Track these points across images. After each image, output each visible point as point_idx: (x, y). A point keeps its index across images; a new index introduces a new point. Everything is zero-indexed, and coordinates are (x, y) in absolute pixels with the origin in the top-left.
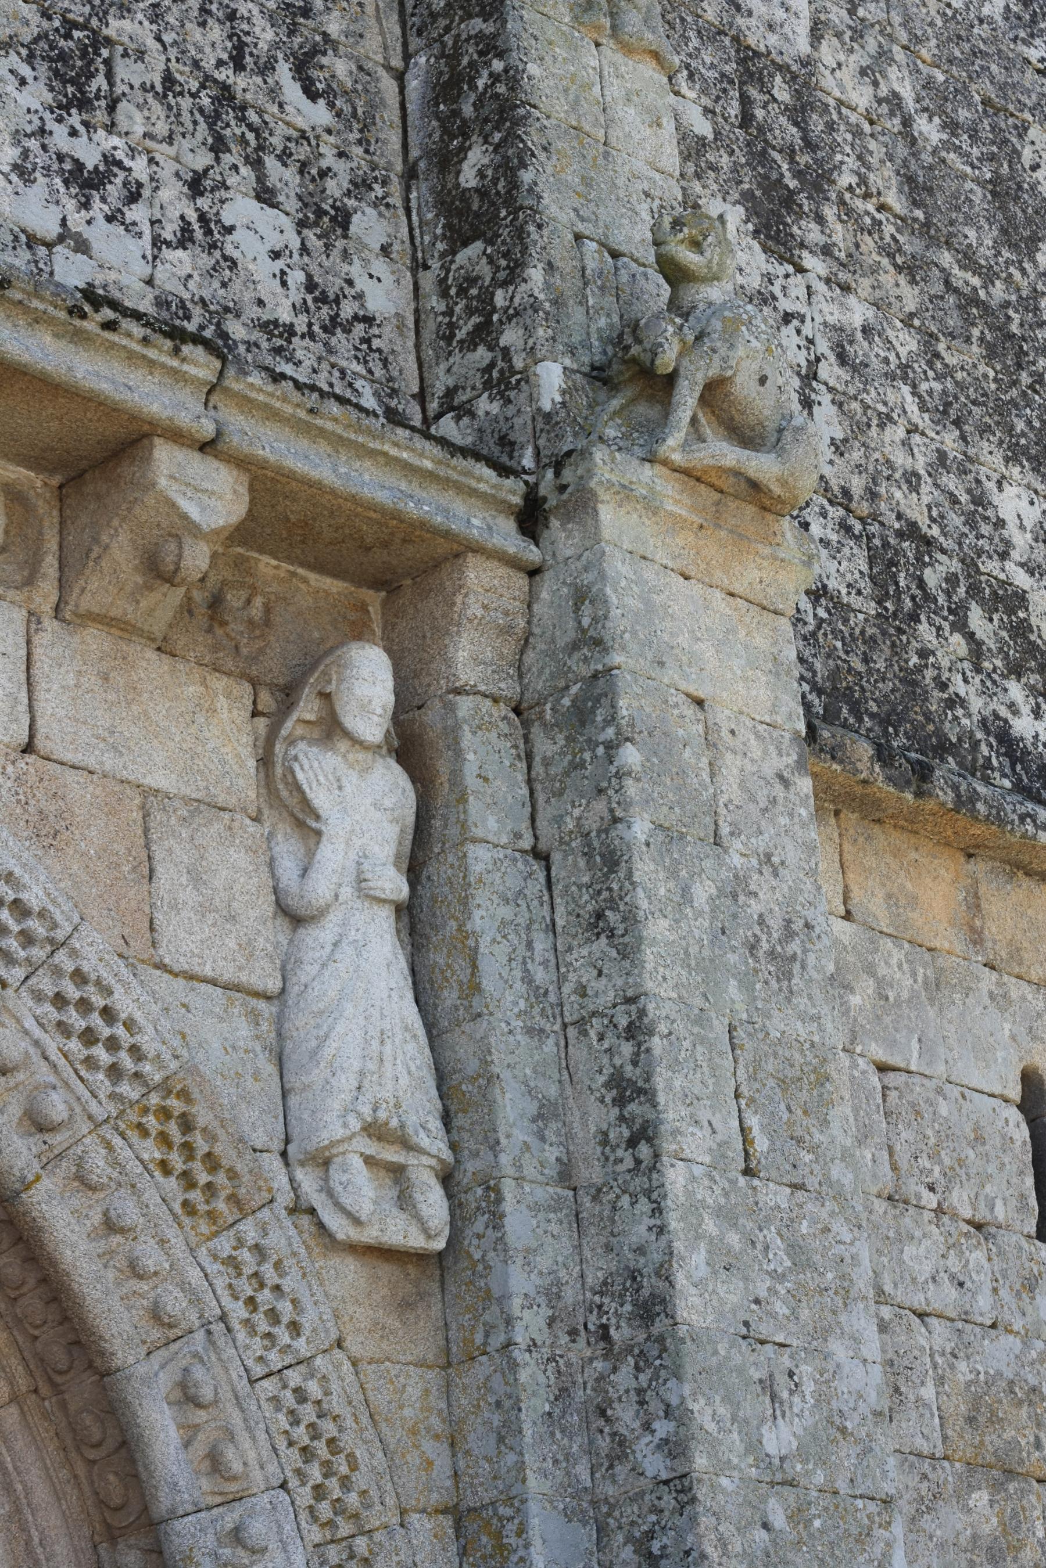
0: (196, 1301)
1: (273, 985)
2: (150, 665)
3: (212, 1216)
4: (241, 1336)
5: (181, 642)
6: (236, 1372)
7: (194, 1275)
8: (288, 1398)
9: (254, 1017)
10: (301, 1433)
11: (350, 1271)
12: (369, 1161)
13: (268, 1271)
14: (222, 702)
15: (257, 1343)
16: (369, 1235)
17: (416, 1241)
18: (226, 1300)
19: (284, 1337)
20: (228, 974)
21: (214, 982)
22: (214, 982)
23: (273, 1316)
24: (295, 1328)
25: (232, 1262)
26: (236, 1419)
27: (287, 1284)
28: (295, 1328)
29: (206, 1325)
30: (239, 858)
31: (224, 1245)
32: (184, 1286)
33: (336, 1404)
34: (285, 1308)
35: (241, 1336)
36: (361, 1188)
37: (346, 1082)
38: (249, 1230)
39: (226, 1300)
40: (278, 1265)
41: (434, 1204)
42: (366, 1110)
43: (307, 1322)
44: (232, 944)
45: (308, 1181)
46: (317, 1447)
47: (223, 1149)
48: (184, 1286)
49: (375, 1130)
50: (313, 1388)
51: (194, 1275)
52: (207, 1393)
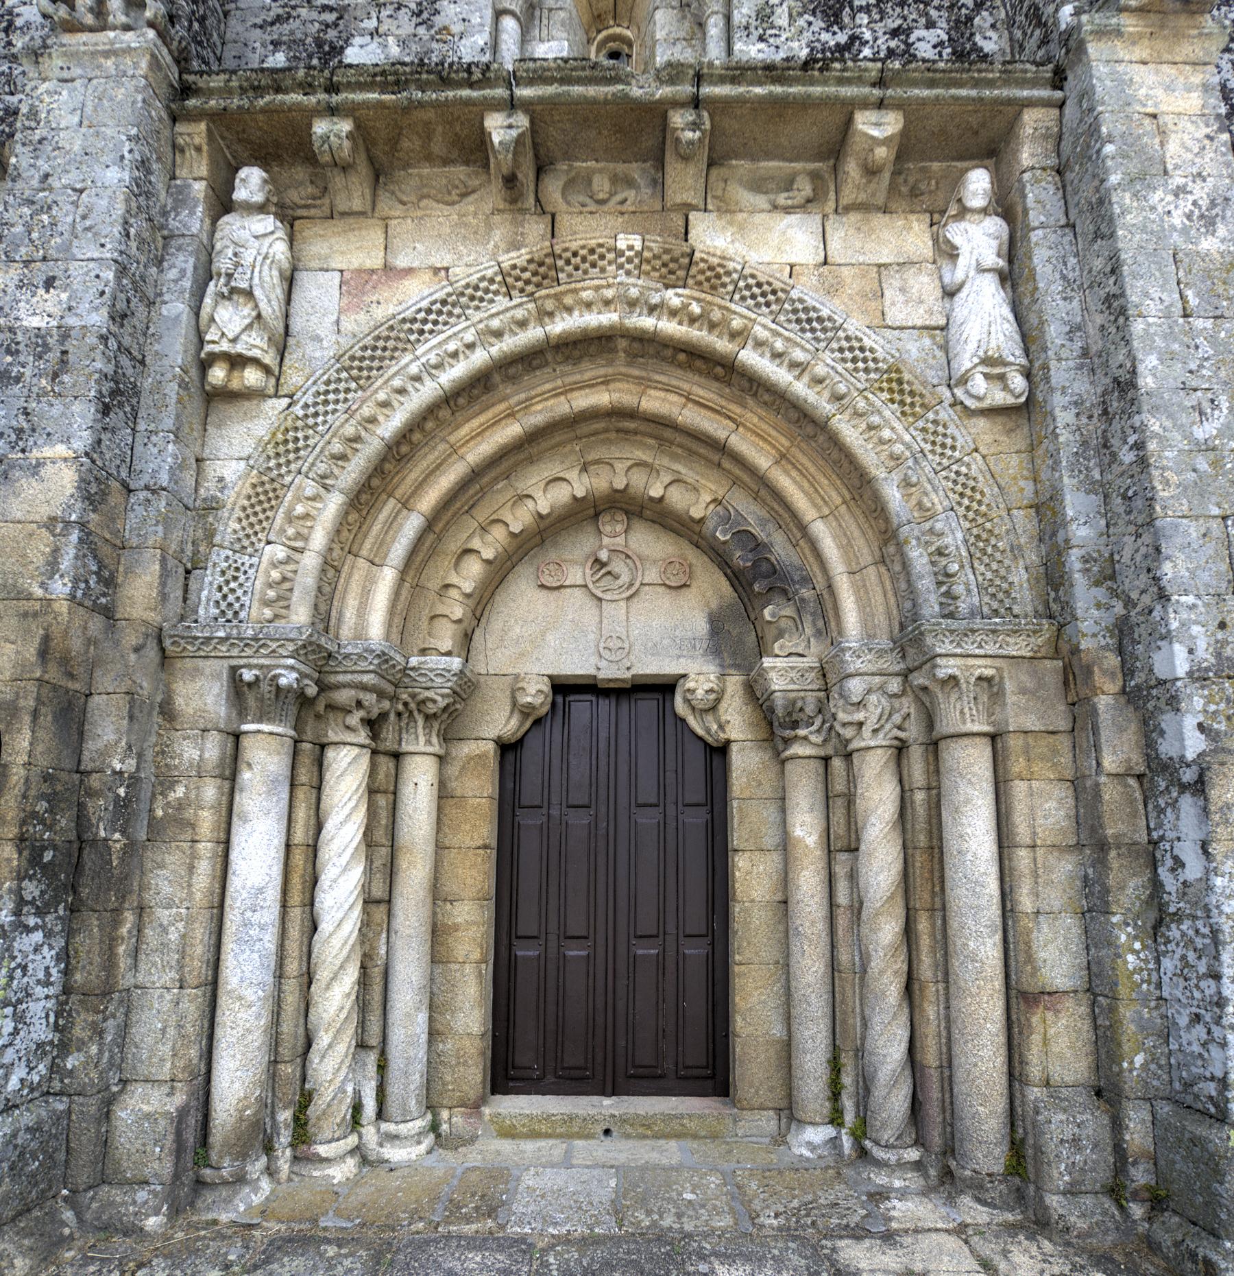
0: (908, 447)
1: (942, 322)
2: (879, 220)
3: (913, 415)
4: (930, 457)
5: (893, 206)
6: (928, 469)
7: (907, 438)
8: (953, 475)
9: (933, 337)
10: (959, 488)
11: (982, 423)
12: (987, 376)
13: (940, 429)
14: (915, 224)
15: (937, 458)
16: (986, 404)
17: (1010, 400)
18: (923, 444)
19: (949, 452)
20: (919, 323)
21: (913, 328)
22: (913, 328)
23: (943, 446)
24: (953, 448)
25: (924, 430)
26: (929, 487)
27: (949, 432)
28: (953, 448)
29: (913, 455)
30: (925, 279)
31: (921, 424)
32: (904, 443)
33: (973, 473)
34: (949, 441)
35: (930, 457)
36: (979, 384)
37: (971, 346)
38: (931, 416)
39: (923, 444)
40: (945, 426)
41: (1018, 382)
42: (981, 353)
43: (958, 445)
44: (921, 311)
45: (959, 392)
46: (965, 489)
47: (917, 387)
48: (904, 443)
49: (987, 361)
50: (964, 470)
51: (907, 438)
52: (914, 479)
